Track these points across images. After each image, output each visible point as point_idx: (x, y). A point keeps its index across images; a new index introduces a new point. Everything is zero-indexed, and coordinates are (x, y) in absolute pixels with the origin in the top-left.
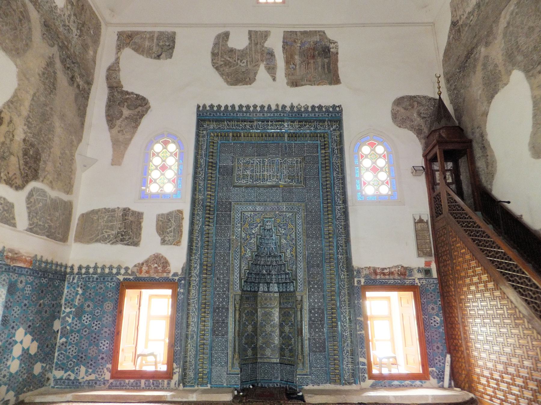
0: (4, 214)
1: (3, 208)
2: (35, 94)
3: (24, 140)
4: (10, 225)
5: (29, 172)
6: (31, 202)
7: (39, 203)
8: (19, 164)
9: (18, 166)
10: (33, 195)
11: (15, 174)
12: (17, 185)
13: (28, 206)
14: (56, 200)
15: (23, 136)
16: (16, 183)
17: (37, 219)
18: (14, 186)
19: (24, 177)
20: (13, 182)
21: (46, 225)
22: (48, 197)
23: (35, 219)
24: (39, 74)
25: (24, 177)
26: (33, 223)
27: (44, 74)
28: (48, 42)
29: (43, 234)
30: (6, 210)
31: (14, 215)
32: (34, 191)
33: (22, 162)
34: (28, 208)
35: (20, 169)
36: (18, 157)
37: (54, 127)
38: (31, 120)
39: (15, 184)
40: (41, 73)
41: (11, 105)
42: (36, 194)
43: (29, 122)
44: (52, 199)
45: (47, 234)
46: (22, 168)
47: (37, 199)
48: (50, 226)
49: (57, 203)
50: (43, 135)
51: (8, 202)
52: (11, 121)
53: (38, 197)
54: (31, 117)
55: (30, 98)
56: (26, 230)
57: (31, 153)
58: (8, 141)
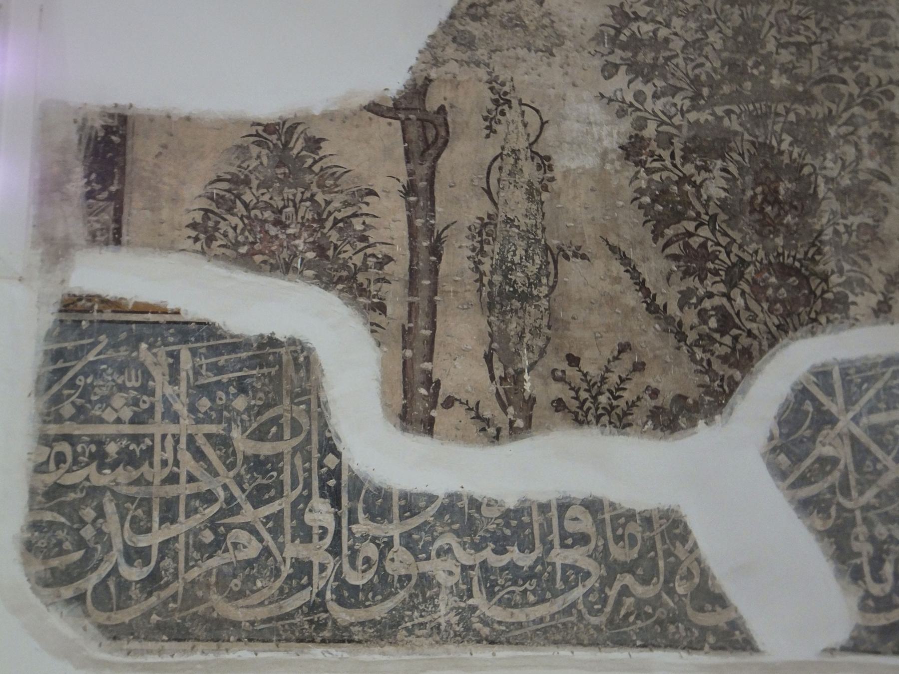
0: (625, 591)
1: (602, 557)
4: (693, 647)
5: (740, 302)
6: (827, 463)
8: (641, 285)
9: (632, 299)
10: (825, 419)
11: (624, 348)
12: (666, 399)
13: (806, 492)
16: (655, 393)
18: (638, 415)
19: (705, 342)
25: (705, 342)
30: (629, 568)
31: (705, 573)
32: (830, 392)
34: (805, 506)
35: (654, 309)
36: (614, 249)
38: (647, 28)
39: (649, 403)
41: (475, 28)
42: (850, 401)
43: (635, 44)
46: (668, 297)
51: (631, 516)
52: (502, 101)
54: (644, 11)
56: (855, 646)
57: (715, 189)
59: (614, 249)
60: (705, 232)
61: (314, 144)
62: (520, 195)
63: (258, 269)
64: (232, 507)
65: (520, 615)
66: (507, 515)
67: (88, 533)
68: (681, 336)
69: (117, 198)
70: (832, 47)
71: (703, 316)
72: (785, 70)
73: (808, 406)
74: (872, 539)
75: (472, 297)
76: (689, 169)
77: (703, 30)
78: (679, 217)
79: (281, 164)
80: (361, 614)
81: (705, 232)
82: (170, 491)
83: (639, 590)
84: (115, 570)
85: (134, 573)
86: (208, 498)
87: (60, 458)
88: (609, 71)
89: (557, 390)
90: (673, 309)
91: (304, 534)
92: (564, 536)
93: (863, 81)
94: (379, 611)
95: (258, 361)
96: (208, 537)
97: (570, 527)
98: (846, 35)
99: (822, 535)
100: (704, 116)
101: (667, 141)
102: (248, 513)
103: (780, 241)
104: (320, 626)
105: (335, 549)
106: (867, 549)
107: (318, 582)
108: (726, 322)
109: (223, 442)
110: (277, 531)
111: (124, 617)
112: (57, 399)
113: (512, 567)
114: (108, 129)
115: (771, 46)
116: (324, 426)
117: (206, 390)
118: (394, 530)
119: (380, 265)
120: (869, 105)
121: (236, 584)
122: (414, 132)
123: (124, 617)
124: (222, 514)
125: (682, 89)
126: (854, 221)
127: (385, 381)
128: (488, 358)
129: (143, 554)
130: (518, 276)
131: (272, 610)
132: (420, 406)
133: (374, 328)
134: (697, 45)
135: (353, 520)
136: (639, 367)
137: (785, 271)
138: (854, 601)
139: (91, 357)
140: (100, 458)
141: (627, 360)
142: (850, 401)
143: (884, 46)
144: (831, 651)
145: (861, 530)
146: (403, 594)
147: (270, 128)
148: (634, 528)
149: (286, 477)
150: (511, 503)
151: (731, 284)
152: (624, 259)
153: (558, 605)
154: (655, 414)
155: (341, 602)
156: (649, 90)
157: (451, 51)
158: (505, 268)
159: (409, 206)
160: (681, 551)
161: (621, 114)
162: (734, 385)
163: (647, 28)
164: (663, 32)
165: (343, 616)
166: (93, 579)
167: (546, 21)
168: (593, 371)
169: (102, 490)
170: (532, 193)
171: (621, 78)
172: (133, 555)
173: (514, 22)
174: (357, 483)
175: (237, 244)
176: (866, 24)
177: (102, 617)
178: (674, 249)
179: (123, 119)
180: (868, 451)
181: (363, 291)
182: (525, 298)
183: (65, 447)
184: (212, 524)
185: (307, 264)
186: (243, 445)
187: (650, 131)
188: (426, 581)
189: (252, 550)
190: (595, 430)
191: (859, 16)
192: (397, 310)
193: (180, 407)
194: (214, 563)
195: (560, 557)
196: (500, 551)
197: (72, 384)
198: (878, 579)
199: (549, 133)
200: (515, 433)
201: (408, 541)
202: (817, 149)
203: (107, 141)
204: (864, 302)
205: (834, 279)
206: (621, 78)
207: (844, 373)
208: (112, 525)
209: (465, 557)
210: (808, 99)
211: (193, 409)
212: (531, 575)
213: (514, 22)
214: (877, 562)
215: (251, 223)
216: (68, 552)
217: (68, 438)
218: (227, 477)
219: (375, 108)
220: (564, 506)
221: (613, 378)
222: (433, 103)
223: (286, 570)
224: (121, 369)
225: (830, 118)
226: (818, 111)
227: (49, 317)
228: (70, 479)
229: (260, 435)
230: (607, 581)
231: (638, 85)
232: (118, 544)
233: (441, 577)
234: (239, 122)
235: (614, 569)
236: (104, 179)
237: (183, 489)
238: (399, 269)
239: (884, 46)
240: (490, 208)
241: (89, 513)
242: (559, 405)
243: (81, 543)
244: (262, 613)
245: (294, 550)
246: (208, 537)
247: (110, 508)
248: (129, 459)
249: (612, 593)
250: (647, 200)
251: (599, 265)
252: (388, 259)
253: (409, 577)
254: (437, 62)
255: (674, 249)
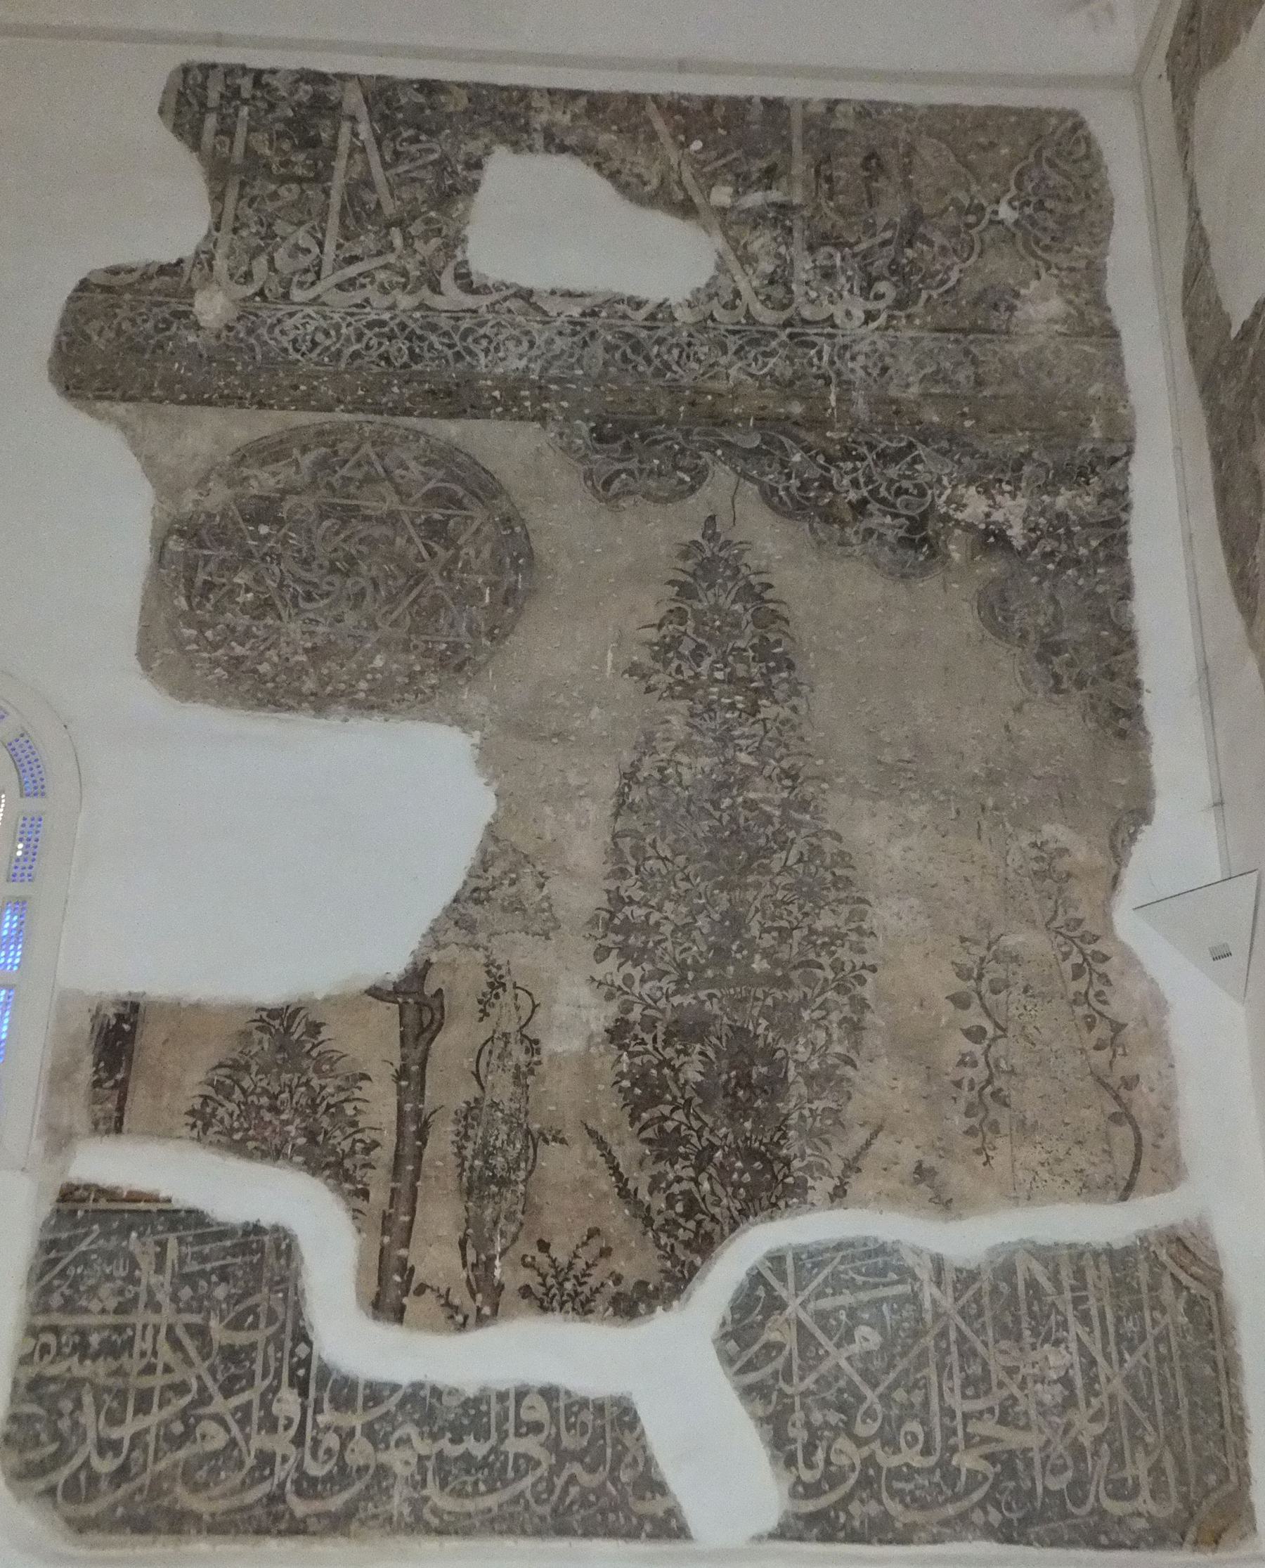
0: (572, 1480)
1: (554, 1445)
2: (630, 777)
3: (618, 1033)
5: (706, 1186)
7: (849, 1337)
8: (615, 1169)
9: (606, 1183)
10: (775, 1305)
11: (593, 1233)
12: (627, 1286)
13: (752, 1378)
14: (1007, 1271)
15: (600, 1016)
16: (618, 1280)
17: (860, 1442)
18: (600, 1303)
19: (671, 1226)
20: (593, 1282)
21: (967, 1461)
22: (925, 1274)
23: (843, 1443)
24: (633, 669)
26: (833, 1478)
27: (665, 649)
28: (647, 495)
29: (958, 1527)
30: (578, 1456)
31: (649, 1461)
32: (782, 1277)
33: (628, 1150)
34: (748, 1393)
35: (625, 1193)
36: (592, 1133)
37: (843, 858)
40: (641, 656)
41: (475, 911)
43: (627, 928)
44: (967, 1278)
45: (995, 1517)
46: (640, 1181)
47: (821, 1316)
48: (1007, 1462)
49: (1032, 1284)
50: (768, 941)
51: (584, 1403)
52: (497, 984)
53: (826, 1304)
54: (638, 895)
55: (597, 812)
56: (782, 1533)
57: (692, 1073)
58: (502, 1087)
59: (592, 1133)
60: (679, 1116)
61: (315, 1028)
62: (507, 1078)
63: (249, 1156)
64: (204, 1398)
65: (469, 1505)
66: (467, 1404)
67: (65, 1424)
68: (648, 1221)
69: (122, 1089)
70: (812, 931)
71: (671, 1201)
72: (766, 954)
73: (761, 1292)
74: (808, 1425)
75: (452, 1184)
76: (669, 1053)
77: (693, 914)
78: (656, 1100)
79: (281, 1049)
80: (317, 1506)
81: (679, 1116)
82: (146, 1382)
83: (586, 1479)
84: (86, 1464)
85: (106, 1466)
86: (180, 1388)
87: (45, 1349)
88: (601, 954)
89: (527, 1277)
90: (644, 1196)
91: (270, 1424)
92: (519, 1423)
93: (838, 967)
94: (336, 1502)
95: (243, 1248)
96: (178, 1428)
97: (526, 1415)
98: (825, 920)
99: (762, 1421)
100: (687, 1000)
101: (649, 1024)
102: (219, 1405)
103: (748, 1125)
104: (277, 1518)
105: (298, 1441)
106: (801, 1435)
107: (280, 1473)
108: (692, 1207)
109: (200, 1333)
110: (244, 1422)
111: (92, 1510)
112: (47, 1290)
113: (467, 1457)
114: (120, 1017)
115: (755, 931)
116: (299, 1314)
117: (188, 1279)
118: (356, 1420)
119: (367, 1150)
120: (841, 988)
121: (201, 1475)
122: (410, 1015)
123: (92, 1510)
124: (194, 1404)
125: (667, 973)
126: (818, 1105)
127: (361, 1268)
128: (462, 1245)
129: (115, 1446)
130: (499, 1161)
131: (235, 1502)
132: (393, 1294)
133: (356, 1213)
134: (686, 929)
135: (318, 1410)
136: (605, 1253)
137: (751, 1155)
138: (785, 1487)
139: (83, 1247)
140: (82, 1349)
141: (596, 1245)
142: (799, 1287)
143: (859, 931)
144: (759, 1538)
145: (798, 1416)
146: (359, 1486)
147: (275, 1013)
148: (588, 1416)
149: (258, 1368)
150: (471, 1392)
151: (699, 1169)
152: (601, 1143)
153: (505, 1495)
154: (616, 1301)
155: (299, 1493)
156: (637, 973)
157: (453, 934)
158: (486, 1152)
159: (400, 1091)
160: (628, 1439)
161: (609, 997)
162: (694, 1269)
163: (640, 912)
164: (655, 917)
165: (300, 1507)
166: (65, 1472)
167: (545, 905)
168: (563, 1260)
169: (83, 1381)
170: (518, 1077)
171: (612, 961)
172: (106, 1446)
173: (515, 906)
174: (325, 1371)
175: (232, 1131)
176: (845, 910)
177: (70, 1509)
178: (649, 1133)
179: (135, 1007)
180: (812, 1336)
181: (348, 1178)
182: (503, 1183)
183: (49, 1339)
184: (183, 1415)
185: (297, 1150)
186: (219, 1333)
187: (635, 1014)
188: (383, 1471)
189: (218, 1440)
190: (558, 1316)
191: (840, 902)
192: (379, 1196)
193: (161, 1297)
194: (182, 1454)
195: (513, 1446)
196: (456, 1440)
197: (63, 1274)
198: (810, 1465)
199: (540, 1015)
200: (481, 1320)
201: (369, 1431)
202: (789, 1033)
203: (117, 1027)
204: (821, 1186)
205: (796, 1164)
206: (612, 961)
207: (797, 1257)
208: (88, 1417)
209: (423, 1447)
210: (786, 983)
211: (175, 1298)
212: (485, 1464)
213: (515, 906)
214: (810, 1448)
215: (247, 1109)
216: (43, 1445)
217: (56, 1330)
218: (202, 1368)
219: (375, 992)
220: (521, 1394)
221: (580, 1264)
222: (430, 989)
223: (250, 1461)
224: (110, 1257)
225: (804, 1002)
226: (794, 995)
227: (47, 1208)
228: (52, 1371)
229: (236, 1325)
230: (554, 1471)
231: (628, 968)
232: (91, 1435)
233: (399, 1468)
234: (243, 1008)
235: (563, 1456)
236: (112, 1069)
237: (158, 1381)
238: (384, 1155)
239: (859, 931)
240: (475, 1091)
241: (66, 1405)
242: (526, 1292)
243: (56, 1436)
244: (222, 1505)
245: (260, 1441)
246: (178, 1428)
247: (88, 1399)
248: (111, 1350)
249: (559, 1482)
250: (626, 1083)
251: (577, 1150)
252: (375, 1144)
253: (367, 1468)
254: (438, 946)
255: (649, 1133)
